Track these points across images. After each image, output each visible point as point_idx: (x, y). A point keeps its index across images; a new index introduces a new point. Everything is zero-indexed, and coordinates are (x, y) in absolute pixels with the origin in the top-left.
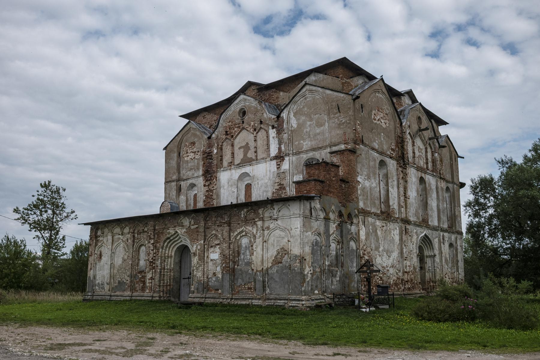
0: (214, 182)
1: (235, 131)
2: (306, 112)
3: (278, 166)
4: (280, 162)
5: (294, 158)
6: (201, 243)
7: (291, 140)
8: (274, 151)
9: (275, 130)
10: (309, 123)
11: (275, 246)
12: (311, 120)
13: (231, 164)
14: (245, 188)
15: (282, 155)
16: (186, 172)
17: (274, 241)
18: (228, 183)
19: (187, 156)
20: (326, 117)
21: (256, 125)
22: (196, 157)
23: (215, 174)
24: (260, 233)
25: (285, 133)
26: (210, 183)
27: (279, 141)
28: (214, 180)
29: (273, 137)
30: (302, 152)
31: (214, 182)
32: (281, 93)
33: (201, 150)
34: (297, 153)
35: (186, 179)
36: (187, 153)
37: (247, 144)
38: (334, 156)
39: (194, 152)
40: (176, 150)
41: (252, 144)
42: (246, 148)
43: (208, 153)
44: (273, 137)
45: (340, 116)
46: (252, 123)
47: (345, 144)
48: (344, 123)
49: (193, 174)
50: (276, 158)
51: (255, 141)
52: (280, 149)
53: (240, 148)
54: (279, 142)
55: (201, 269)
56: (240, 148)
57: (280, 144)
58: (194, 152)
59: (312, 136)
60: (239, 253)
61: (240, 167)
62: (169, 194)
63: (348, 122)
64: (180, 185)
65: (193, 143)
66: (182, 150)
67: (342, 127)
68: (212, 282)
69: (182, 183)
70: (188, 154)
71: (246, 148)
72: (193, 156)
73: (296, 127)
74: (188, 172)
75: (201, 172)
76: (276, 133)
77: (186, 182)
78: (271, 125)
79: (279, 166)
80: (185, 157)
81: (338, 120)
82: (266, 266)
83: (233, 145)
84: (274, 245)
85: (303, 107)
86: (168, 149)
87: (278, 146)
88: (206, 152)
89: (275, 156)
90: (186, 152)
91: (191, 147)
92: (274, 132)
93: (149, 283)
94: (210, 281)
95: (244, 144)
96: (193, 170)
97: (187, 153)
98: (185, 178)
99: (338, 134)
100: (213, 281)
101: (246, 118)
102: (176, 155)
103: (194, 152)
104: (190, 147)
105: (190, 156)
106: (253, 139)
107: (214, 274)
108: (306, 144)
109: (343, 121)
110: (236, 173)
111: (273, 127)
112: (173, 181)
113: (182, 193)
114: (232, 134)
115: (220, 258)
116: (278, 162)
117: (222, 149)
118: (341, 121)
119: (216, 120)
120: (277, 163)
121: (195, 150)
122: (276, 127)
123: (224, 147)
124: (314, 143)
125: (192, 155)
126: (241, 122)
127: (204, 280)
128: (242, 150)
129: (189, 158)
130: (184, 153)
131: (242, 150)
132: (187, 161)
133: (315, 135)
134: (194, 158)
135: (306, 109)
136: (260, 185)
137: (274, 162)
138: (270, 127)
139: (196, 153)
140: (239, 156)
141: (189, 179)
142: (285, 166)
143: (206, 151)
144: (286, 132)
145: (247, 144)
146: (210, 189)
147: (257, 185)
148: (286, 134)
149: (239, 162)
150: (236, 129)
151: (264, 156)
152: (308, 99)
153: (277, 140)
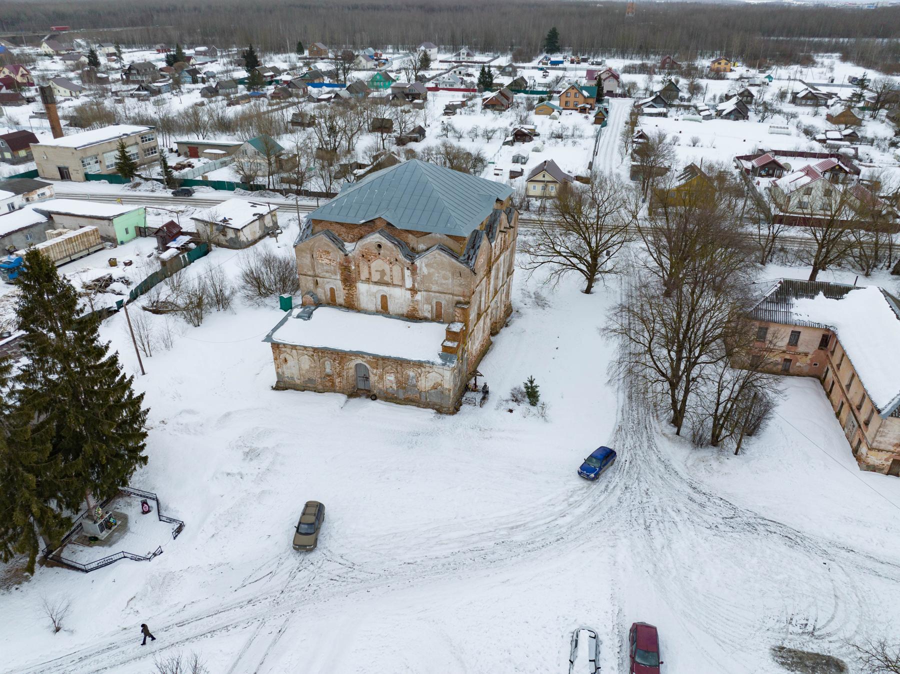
5: (424, 293)
7: (422, 282)
8: (409, 283)
12: (439, 273)
13: (368, 280)
20: (450, 275)
37: (383, 270)
40: (308, 252)
46: (388, 258)
50: (410, 290)
51: (391, 271)
53: (376, 271)
56: (376, 271)
57: (414, 281)
58: (330, 260)
60: (408, 379)
65: (328, 253)
66: (314, 253)
69: (318, 279)
75: (339, 277)
82: (427, 389)
83: (370, 267)
86: (298, 247)
101: (382, 252)
102: (309, 256)
106: (389, 270)
107: (391, 387)
108: (434, 288)
110: (375, 288)
111: (408, 269)
112: (310, 276)
117: (359, 266)
121: (330, 258)
123: (360, 265)
124: (440, 289)
125: (327, 261)
133: (442, 284)
137: (409, 292)
140: (376, 277)
142: (418, 297)
145: (383, 270)
149: (376, 280)
151: (400, 284)
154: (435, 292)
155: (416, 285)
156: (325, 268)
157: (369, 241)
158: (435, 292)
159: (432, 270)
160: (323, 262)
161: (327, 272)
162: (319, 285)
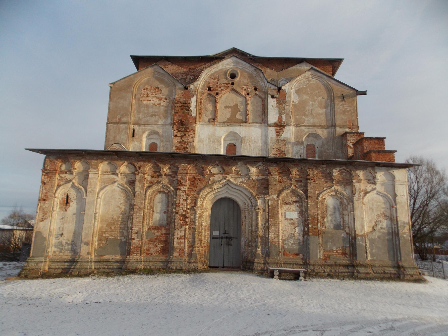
0: (191, 134)
1: (222, 90)
2: (309, 93)
3: (277, 134)
4: (280, 130)
6: (273, 198)
9: (275, 100)
10: (311, 103)
11: (374, 211)
13: (213, 120)
14: (227, 147)
15: (282, 124)
16: (145, 117)
17: (373, 205)
18: (209, 139)
19: (148, 100)
21: (250, 90)
22: (162, 104)
23: (191, 127)
24: (359, 195)
25: (287, 105)
26: (185, 135)
27: (279, 111)
28: (191, 133)
29: (273, 106)
30: (304, 126)
31: (191, 134)
32: (268, 70)
33: (171, 98)
34: (298, 126)
35: (144, 125)
36: (148, 96)
37: (237, 105)
38: (352, 136)
39: (160, 99)
41: (241, 108)
42: (235, 109)
43: (183, 103)
44: (273, 106)
45: (345, 104)
46: (245, 87)
47: (350, 128)
48: (349, 111)
49: (157, 121)
50: (276, 125)
52: (280, 118)
53: (226, 107)
54: (279, 111)
55: (273, 229)
56: (226, 107)
59: (315, 115)
61: (228, 125)
62: (115, 137)
63: (352, 111)
64: (134, 130)
67: (346, 113)
68: (289, 245)
70: (149, 99)
71: (235, 109)
72: (156, 102)
73: (297, 102)
74: (148, 118)
76: (276, 102)
77: (143, 127)
78: (270, 94)
79: (278, 134)
80: (144, 100)
81: (343, 107)
84: (373, 210)
85: (307, 88)
87: (278, 115)
88: (180, 102)
89: (275, 124)
90: (146, 95)
91: (155, 92)
92: (274, 102)
93: (178, 243)
94: (286, 244)
95: (232, 104)
96: (157, 117)
97: (148, 96)
98: (142, 122)
99: (343, 119)
100: (290, 244)
101: (237, 80)
103: (159, 98)
104: (151, 91)
105: (152, 101)
109: (348, 109)
111: (273, 97)
113: (136, 139)
114: (217, 92)
115: (300, 217)
116: (277, 130)
118: (346, 109)
119: (184, 73)
120: (276, 130)
121: (160, 96)
122: (276, 98)
125: (156, 101)
126: (231, 83)
127: (279, 242)
128: (230, 109)
129: (150, 103)
130: (142, 96)
131: (230, 109)
132: (147, 106)
134: (158, 104)
135: (309, 90)
136: (252, 147)
138: (270, 96)
139: (163, 100)
141: (150, 125)
143: (179, 100)
144: (288, 104)
146: (183, 141)
147: (248, 147)
148: (288, 106)
150: (222, 88)
152: (311, 82)
153: (276, 110)
154: (309, 126)
155: (284, 118)
156: (151, 110)
157: (220, 67)
158: (309, 126)
159: (305, 97)
160: (150, 103)
161: (152, 115)
162: (136, 136)
